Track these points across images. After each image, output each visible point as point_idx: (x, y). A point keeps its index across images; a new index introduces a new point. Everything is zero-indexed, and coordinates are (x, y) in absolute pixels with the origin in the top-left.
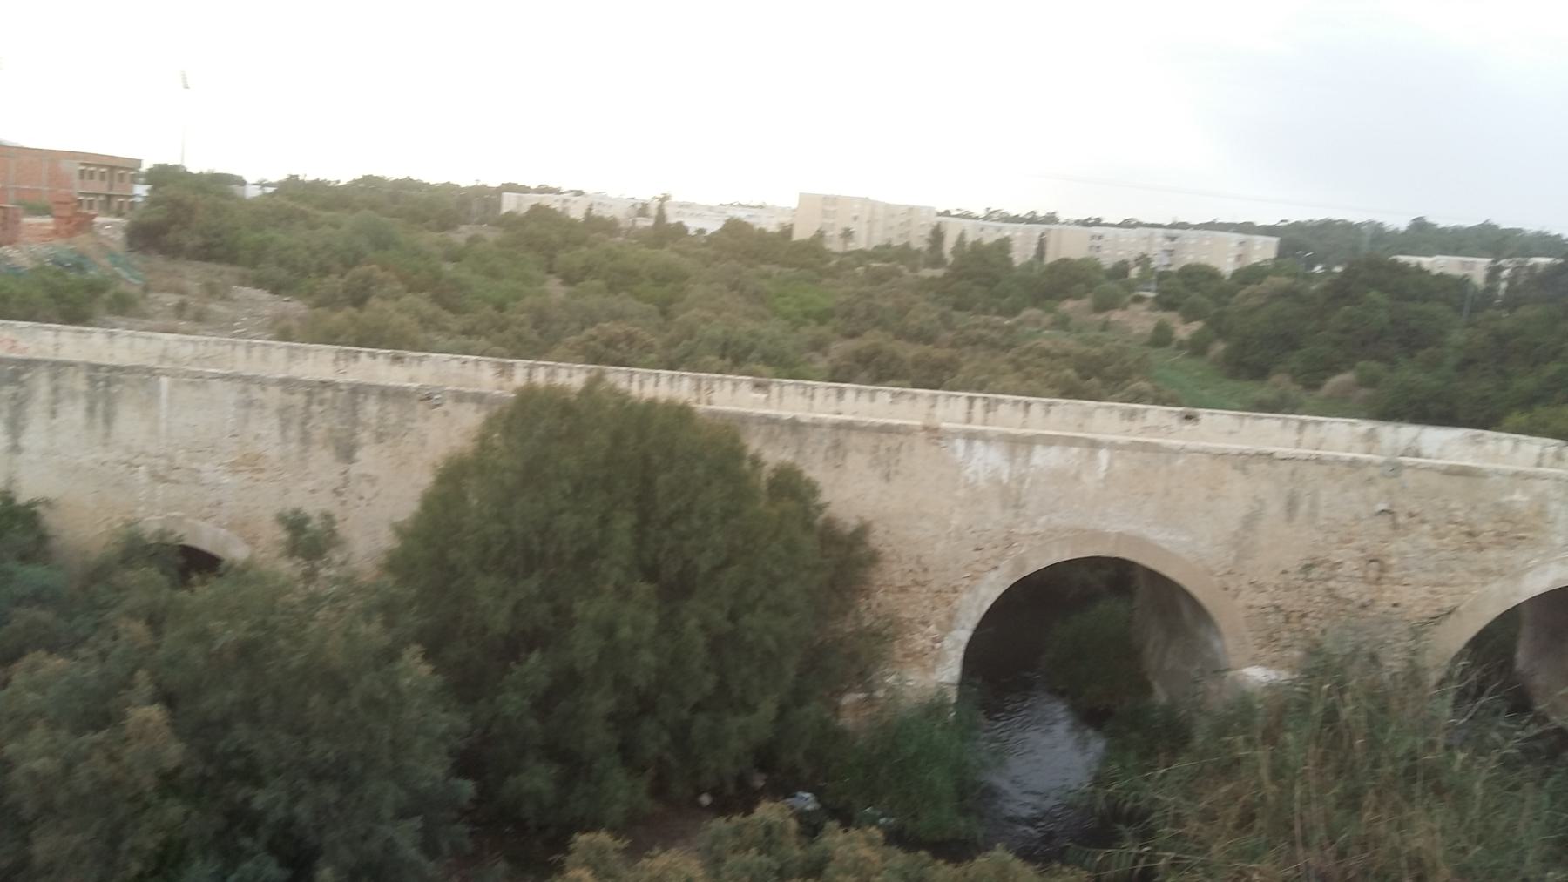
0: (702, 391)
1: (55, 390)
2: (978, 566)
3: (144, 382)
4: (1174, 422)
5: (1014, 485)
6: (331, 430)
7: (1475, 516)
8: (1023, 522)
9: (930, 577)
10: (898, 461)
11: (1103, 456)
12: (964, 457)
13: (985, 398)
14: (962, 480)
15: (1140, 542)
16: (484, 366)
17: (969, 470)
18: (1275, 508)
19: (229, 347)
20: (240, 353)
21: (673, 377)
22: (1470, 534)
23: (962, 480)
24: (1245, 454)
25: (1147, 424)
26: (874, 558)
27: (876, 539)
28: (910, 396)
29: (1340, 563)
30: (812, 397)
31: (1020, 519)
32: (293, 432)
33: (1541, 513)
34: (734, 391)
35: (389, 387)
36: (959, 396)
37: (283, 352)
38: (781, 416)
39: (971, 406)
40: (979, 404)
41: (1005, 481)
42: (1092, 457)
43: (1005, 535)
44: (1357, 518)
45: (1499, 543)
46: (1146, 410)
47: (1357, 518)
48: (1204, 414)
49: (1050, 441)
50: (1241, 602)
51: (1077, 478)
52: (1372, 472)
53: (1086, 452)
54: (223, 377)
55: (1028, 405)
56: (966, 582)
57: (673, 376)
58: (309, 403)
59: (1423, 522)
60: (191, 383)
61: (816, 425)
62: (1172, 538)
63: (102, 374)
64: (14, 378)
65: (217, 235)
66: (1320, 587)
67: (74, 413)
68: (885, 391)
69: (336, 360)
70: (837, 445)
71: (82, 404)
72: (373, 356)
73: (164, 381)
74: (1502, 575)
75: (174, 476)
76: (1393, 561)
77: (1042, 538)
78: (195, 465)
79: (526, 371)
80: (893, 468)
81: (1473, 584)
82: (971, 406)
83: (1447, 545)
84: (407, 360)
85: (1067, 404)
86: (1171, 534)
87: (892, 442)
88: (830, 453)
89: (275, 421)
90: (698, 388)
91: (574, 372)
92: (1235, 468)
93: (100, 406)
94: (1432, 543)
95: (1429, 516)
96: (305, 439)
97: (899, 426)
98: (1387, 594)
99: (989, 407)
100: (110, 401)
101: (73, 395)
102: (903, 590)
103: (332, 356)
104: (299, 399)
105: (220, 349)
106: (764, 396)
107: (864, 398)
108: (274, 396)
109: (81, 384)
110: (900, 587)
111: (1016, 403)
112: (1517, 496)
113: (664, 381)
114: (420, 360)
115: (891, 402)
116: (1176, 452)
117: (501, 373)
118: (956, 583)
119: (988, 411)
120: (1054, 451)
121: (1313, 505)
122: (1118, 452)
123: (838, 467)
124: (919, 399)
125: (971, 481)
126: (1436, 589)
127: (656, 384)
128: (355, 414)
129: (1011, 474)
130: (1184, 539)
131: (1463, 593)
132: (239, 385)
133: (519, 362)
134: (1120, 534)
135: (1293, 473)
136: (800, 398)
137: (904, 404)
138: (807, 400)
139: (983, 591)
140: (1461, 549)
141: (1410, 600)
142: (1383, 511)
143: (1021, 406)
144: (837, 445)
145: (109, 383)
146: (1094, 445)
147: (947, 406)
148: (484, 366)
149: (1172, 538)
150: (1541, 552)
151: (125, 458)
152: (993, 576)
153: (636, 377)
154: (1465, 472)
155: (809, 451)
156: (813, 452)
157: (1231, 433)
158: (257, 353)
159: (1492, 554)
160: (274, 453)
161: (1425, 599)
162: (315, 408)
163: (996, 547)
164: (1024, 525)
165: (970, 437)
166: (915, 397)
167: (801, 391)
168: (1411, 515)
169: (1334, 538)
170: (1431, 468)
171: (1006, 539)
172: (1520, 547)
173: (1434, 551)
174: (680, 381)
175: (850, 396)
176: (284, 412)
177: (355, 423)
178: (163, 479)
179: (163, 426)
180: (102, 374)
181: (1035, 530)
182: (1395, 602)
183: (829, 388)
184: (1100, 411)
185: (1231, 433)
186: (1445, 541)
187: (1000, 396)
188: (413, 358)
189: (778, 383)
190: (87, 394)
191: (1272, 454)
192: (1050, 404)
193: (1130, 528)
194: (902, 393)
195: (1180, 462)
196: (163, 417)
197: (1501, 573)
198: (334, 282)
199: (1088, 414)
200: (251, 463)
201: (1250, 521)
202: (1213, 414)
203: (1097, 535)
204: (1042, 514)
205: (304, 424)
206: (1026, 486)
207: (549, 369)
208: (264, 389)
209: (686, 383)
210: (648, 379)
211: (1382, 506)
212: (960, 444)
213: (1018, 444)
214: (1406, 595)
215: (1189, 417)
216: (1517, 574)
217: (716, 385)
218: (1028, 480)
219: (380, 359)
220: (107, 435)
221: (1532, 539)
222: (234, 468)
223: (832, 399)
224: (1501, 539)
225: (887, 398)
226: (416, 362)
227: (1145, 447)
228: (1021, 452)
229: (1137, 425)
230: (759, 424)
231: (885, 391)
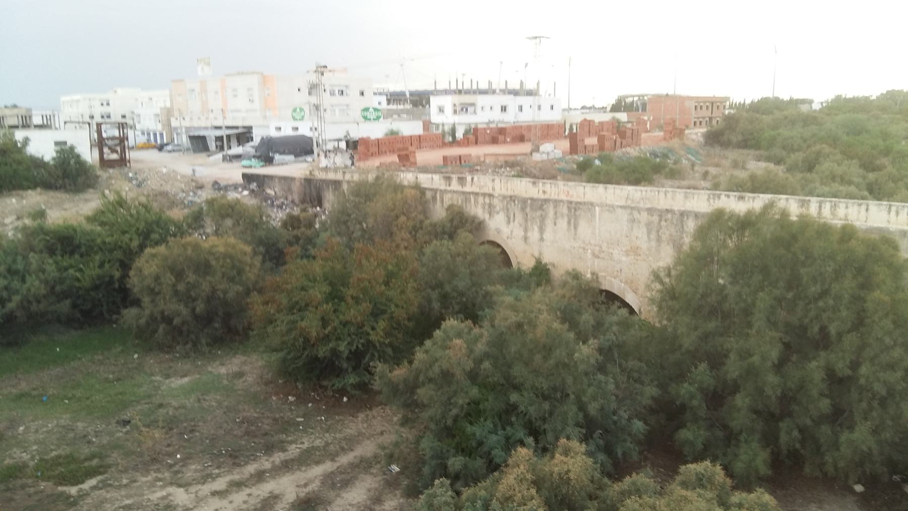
1: (556, 213)
3: (589, 210)
6: (671, 235)
19: (657, 193)
20: (662, 195)
32: (653, 236)
35: (700, 213)
37: (683, 195)
54: (621, 207)
58: (660, 221)
60: (608, 210)
63: (573, 205)
64: (541, 208)
65: (751, 134)
67: (563, 223)
69: (708, 200)
71: (566, 219)
72: (728, 196)
73: (597, 208)
75: (602, 255)
78: (611, 251)
79: (818, 204)
84: (746, 198)
89: (645, 230)
93: (572, 221)
96: (659, 240)
100: (576, 218)
101: (562, 216)
103: (706, 197)
104: (655, 218)
105: (653, 194)
108: (644, 216)
109: (565, 211)
114: (754, 198)
117: (802, 206)
128: (683, 227)
132: (629, 211)
145: (575, 210)
151: (582, 245)
153: (894, 209)
158: (669, 195)
160: (644, 246)
162: (663, 223)
176: (649, 225)
177: (683, 231)
178: (598, 257)
179: (597, 231)
180: (573, 205)
188: (749, 197)
190: (568, 216)
196: (597, 226)
198: (798, 157)
200: (634, 251)
205: (658, 231)
207: (833, 204)
208: (639, 213)
219: (732, 198)
220: (576, 234)
222: (627, 253)
226: (751, 200)
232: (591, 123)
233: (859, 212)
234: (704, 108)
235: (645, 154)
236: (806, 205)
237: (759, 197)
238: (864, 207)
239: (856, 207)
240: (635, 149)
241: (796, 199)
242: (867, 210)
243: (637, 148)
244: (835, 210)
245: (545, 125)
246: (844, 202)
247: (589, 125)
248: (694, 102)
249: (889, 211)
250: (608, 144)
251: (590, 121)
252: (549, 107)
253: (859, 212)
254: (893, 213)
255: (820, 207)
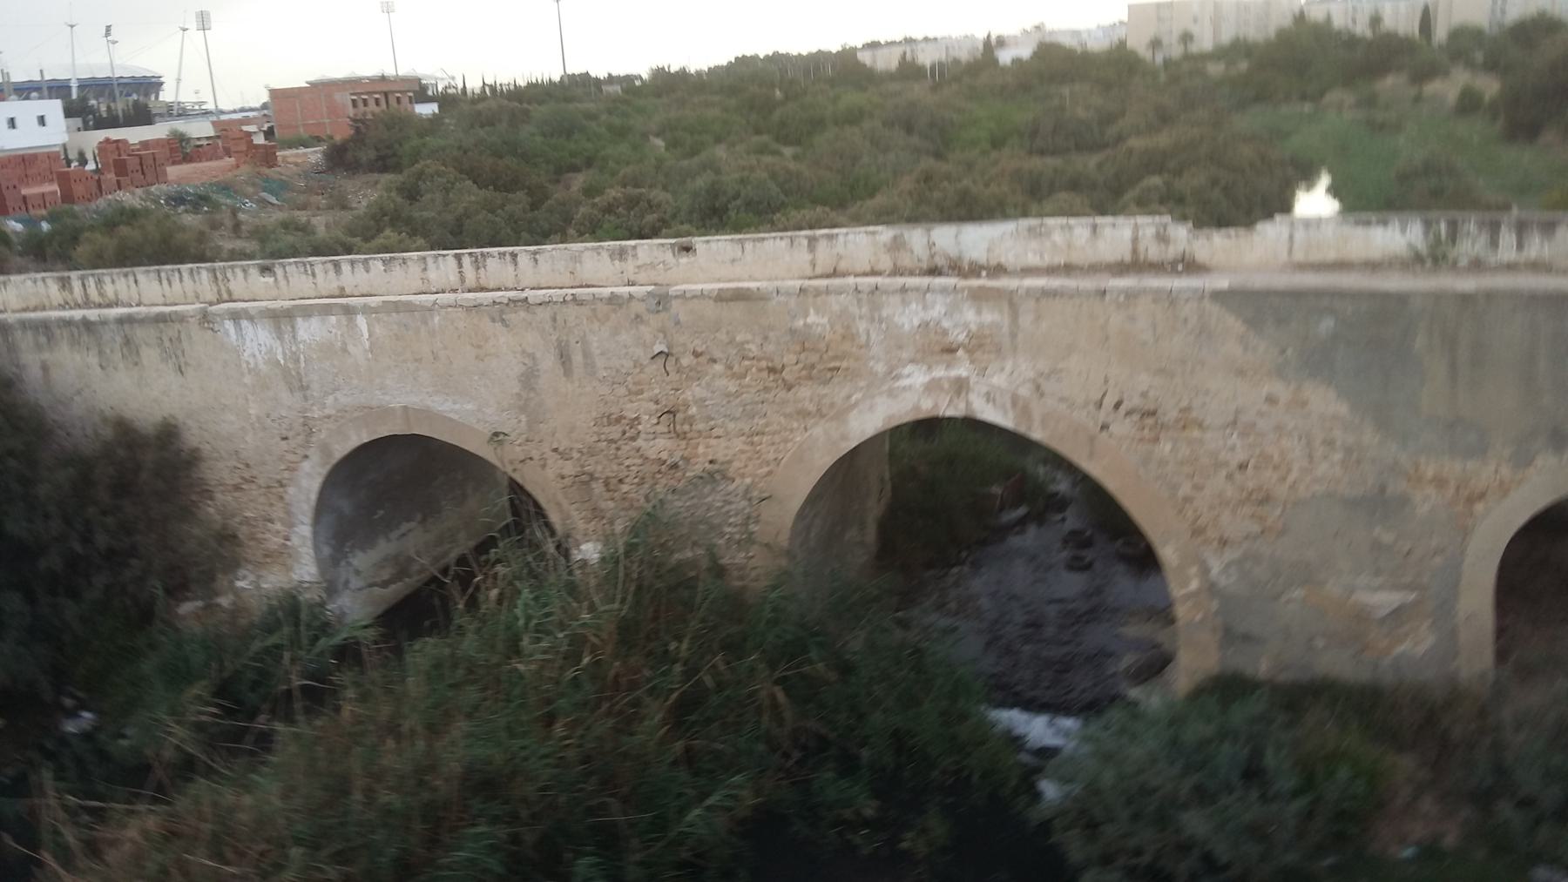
0: (220, 283)
2: (291, 457)
4: (669, 256)
5: (291, 366)
7: (770, 348)
8: (312, 405)
9: (255, 473)
10: (183, 352)
11: (361, 321)
12: (237, 340)
13: (470, 254)
14: (244, 365)
15: (427, 414)
16: (50, 282)
17: (245, 354)
18: (548, 362)
21: (191, 270)
22: (772, 370)
23: (244, 365)
24: (500, 303)
25: (640, 262)
26: (193, 459)
27: (193, 437)
28: (401, 261)
29: (637, 418)
30: (314, 275)
31: (311, 402)
33: (849, 336)
34: (245, 278)
36: (444, 256)
38: (73, 317)
39: (460, 265)
40: (466, 261)
41: (282, 362)
42: (352, 325)
43: (302, 420)
44: (637, 364)
45: (810, 378)
46: (634, 247)
47: (637, 364)
48: (698, 242)
49: (307, 312)
50: (550, 473)
51: (345, 350)
52: (637, 307)
53: (344, 319)
55: (514, 256)
56: (286, 474)
57: (192, 270)
59: (714, 361)
61: (104, 322)
62: (457, 407)
65: (388, 147)
66: (628, 448)
68: (375, 259)
70: (127, 342)
74: (823, 416)
76: (693, 410)
77: (337, 421)
79: (80, 282)
80: (182, 360)
81: (792, 430)
82: (460, 265)
83: (749, 386)
85: (553, 249)
86: (455, 403)
87: (171, 330)
88: (125, 350)
90: (216, 278)
91: (115, 277)
92: (493, 320)
94: (732, 387)
95: (717, 354)
97: (170, 314)
98: (701, 449)
99: (478, 264)
102: (237, 488)
106: (272, 279)
107: (360, 268)
110: (234, 485)
111: (502, 255)
112: (812, 319)
113: (186, 275)
115: (385, 271)
116: (431, 309)
117: (63, 287)
118: (279, 477)
119: (478, 268)
120: (315, 322)
121: (586, 354)
122: (374, 315)
123: (136, 364)
124: (409, 263)
125: (252, 366)
126: (756, 439)
127: (181, 280)
129: (284, 354)
130: (469, 407)
131: (786, 441)
133: (74, 275)
134: (405, 408)
135: (554, 320)
136: (304, 277)
137: (397, 271)
138: (311, 277)
139: (304, 483)
140: (767, 389)
141: (726, 455)
142: (661, 352)
143: (508, 257)
144: (127, 342)
146: (349, 311)
147: (438, 268)
148: (50, 282)
149: (457, 407)
150: (862, 384)
152: (306, 465)
153: (163, 275)
154: (740, 296)
155: (108, 351)
156: (112, 351)
157: (733, 261)
159: (804, 392)
161: (742, 452)
163: (299, 434)
164: (315, 408)
165: (236, 316)
166: (404, 261)
167: (302, 269)
168: (696, 354)
169: (622, 391)
170: (702, 295)
171: (305, 425)
172: (835, 380)
173: (737, 394)
174: (199, 273)
175: (346, 268)
181: (327, 412)
182: (710, 458)
183: (325, 262)
184: (587, 254)
185: (733, 261)
186: (748, 379)
187: (485, 250)
189: (279, 264)
191: (527, 298)
192: (535, 253)
193: (414, 400)
194: (391, 258)
195: (437, 319)
197: (820, 414)
199: (576, 259)
201: (529, 379)
202: (708, 242)
203: (385, 412)
204: (327, 394)
206: (303, 365)
209: (204, 274)
210: (173, 275)
211: (658, 348)
212: (229, 325)
213: (281, 319)
214: (720, 450)
215: (687, 249)
216: (841, 414)
217: (229, 275)
218: (302, 356)
221: (847, 369)
223: (332, 274)
224: (810, 373)
225: (379, 265)
227: (397, 307)
228: (286, 328)
229: (630, 266)
230: (59, 327)
231: (375, 259)
232: (120, 145)
233: (129, 287)
234: (372, 103)
235: (156, 202)
236: (67, 285)
237: (10, 280)
238: (131, 279)
239: (123, 279)
240: (133, 194)
241: (53, 277)
242: (136, 282)
243: (139, 191)
244: (102, 288)
245: (16, 157)
246: (108, 274)
247: (118, 148)
248: (348, 93)
249: (160, 281)
250: (79, 189)
251: (117, 141)
252: (35, 121)
253: (129, 287)
254: (165, 282)
255: (84, 285)
